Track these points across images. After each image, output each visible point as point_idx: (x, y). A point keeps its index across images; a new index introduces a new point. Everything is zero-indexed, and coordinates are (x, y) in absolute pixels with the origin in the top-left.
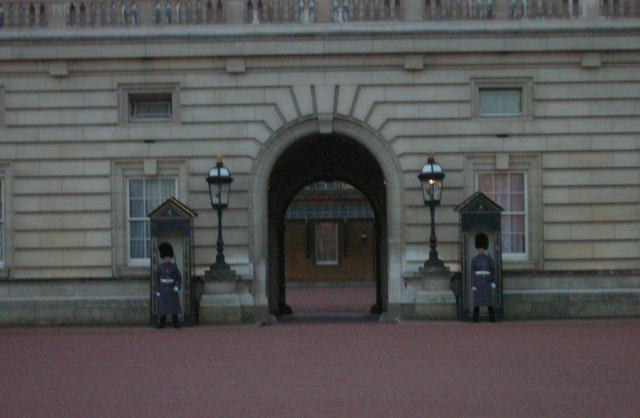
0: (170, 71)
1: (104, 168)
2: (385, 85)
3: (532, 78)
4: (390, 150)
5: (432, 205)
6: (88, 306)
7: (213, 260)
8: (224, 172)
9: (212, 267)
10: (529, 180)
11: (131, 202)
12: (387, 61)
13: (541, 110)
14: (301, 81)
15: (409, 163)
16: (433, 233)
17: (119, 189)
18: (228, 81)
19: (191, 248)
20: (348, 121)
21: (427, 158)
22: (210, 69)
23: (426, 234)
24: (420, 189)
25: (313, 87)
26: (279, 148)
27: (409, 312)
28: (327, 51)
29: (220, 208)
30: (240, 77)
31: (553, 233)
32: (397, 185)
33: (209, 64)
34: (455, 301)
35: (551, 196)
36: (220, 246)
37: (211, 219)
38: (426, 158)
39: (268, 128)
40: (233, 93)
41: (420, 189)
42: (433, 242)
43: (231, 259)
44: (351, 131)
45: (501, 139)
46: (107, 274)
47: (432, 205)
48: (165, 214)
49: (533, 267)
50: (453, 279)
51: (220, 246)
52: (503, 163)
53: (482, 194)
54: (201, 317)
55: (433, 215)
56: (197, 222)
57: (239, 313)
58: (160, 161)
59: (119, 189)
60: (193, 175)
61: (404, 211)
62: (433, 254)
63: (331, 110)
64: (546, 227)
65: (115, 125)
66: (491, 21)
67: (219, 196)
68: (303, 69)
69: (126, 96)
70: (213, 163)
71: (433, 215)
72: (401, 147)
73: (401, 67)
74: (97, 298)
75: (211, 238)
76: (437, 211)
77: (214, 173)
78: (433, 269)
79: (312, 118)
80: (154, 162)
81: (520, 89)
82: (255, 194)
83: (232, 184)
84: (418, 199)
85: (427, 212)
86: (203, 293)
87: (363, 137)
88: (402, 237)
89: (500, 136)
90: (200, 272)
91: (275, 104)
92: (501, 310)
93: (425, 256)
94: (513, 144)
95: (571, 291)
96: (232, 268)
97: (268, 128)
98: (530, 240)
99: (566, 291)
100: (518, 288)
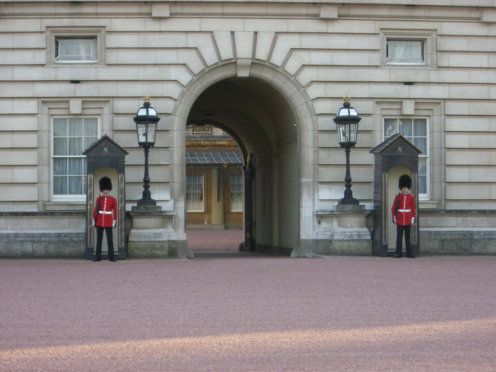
0: (97, 15)
1: (32, 107)
2: (300, 33)
3: (436, 30)
4: (304, 94)
6: (20, 239)
7: (141, 197)
8: (152, 113)
9: (139, 202)
10: (432, 125)
11: (54, 139)
12: (304, 11)
15: (322, 107)
16: (348, 173)
17: (45, 128)
18: (151, 25)
21: (343, 102)
23: (341, 174)
24: (335, 131)
25: (232, 32)
27: (325, 248)
31: (454, 175)
34: (369, 237)
35: (453, 141)
36: (146, 183)
38: (342, 103)
39: (190, 71)
40: (157, 36)
42: (348, 182)
44: (267, 75)
45: (407, 86)
46: (34, 209)
47: (348, 146)
49: (434, 206)
50: (368, 216)
51: (146, 183)
52: (409, 109)
53: (401, 138)
54: (130, 252)
55: (348, 156)
57: (166, 248)
58: (86, 101)
59: (45, 128)
60: (117, 114)
61: (316, 153)
62: (348, 193)
63: (250, 56)
64: (448, 170)
65: (43, 65)
67: (146, 135)
68: (223, 15)
69: (54, 37)
70: (141, 103)
71: (348, 156)
72: (315, 91)
73: (316, 17)
74: (29, 232)
75: (139, 175)
76: (353, 152)
77: (142, 113)
78: (349, 207)
79: (232, 63)
80: (79, 102)
81: (423, 41)
83: (159, 123)
85: (343, 152)
86: (132, 228)
87: (278, 81)
88: (314, 177)
89: (406, 83)
91: (196, 48)
92: (418, 246)
93: (341, 196)
94: (418, 92)
95: (475, 229)
96: (158, 204)
97: (190, 71)
98: (432, 182)
99: (470, 229)
100: (427, 227)
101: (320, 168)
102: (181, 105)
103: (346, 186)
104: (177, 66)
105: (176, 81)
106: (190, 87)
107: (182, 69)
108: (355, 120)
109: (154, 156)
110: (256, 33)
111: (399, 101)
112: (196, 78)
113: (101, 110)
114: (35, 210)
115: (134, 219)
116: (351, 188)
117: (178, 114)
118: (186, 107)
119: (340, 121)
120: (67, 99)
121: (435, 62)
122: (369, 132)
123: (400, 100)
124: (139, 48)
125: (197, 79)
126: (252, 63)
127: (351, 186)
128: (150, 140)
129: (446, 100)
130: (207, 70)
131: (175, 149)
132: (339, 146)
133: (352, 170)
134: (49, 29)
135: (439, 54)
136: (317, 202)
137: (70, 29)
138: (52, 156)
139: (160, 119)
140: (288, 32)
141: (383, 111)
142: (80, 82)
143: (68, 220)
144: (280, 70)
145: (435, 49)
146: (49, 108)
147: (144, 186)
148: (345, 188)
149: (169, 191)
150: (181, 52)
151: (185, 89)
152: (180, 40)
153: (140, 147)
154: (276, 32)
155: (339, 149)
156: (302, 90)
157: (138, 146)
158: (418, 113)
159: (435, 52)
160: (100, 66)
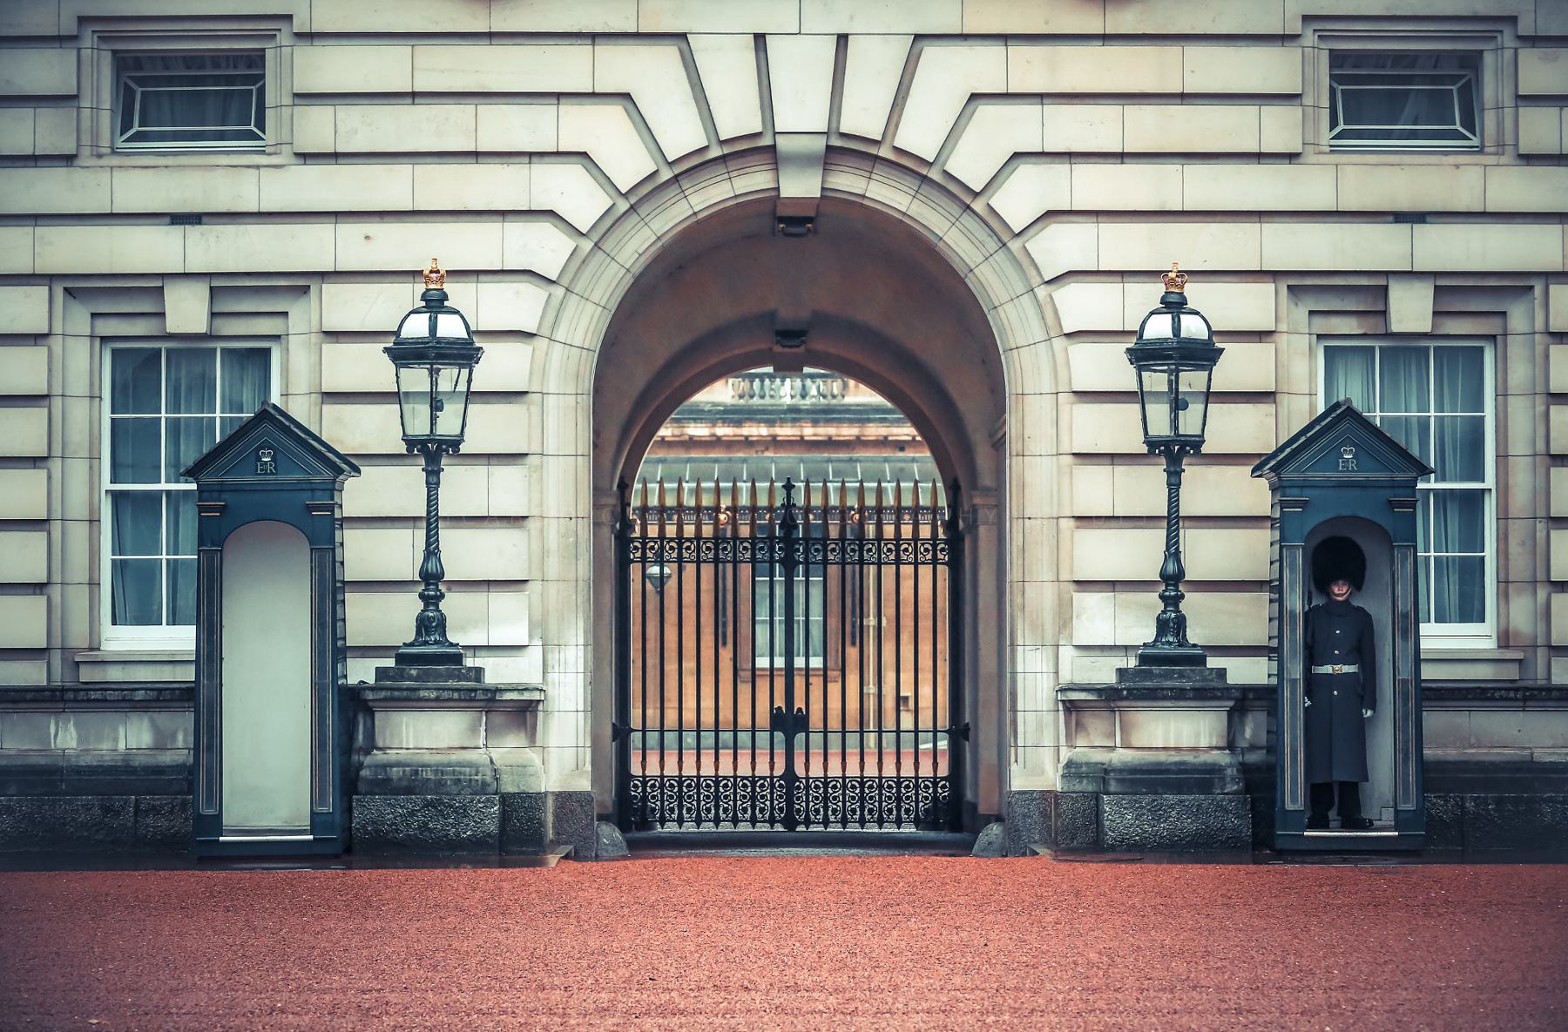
5: (1175, 452)
8: (450, 327)
15: (1084, 305)
16: (1173, 551)
19: (330, 592)
20: (876, 159)
24: (1139, 396)
25: (760, 39)
26: (638, 244)
29: (432, 452)
36: (431, 581)
37: (401, 489)
38: (1157, 290)
41: (1139, 396)
43: (470, 622)
47: (1175, 452)
49: (1511, 672)
51: (431, 581)
56: (357, 496)
62: (1172, 625)
70: (411, 294)
77: (417, 327)
79: (758, 150)
83: (477, 368)
84: (1119, 428)
90: (361, 672)
96: (469, 662)
97: (606, 181)
103: (1161, 597)
105: (551, 213)
107: (576, 170)
108: (1202, 354)
109: (462, 488)
111: (152, 286)
112: (623, 206)
115: (378, 716)
116: (1183, 606)
122: (518, 398)
125: (632, 207)
126: (829, 149)
132: (1145, 449)
136: (1067, 653)
138: (107, 484)
142: (204, 219)
146: (93, 315)
147: (421, 596)
154: (918, 37)
156: (1015, 245)
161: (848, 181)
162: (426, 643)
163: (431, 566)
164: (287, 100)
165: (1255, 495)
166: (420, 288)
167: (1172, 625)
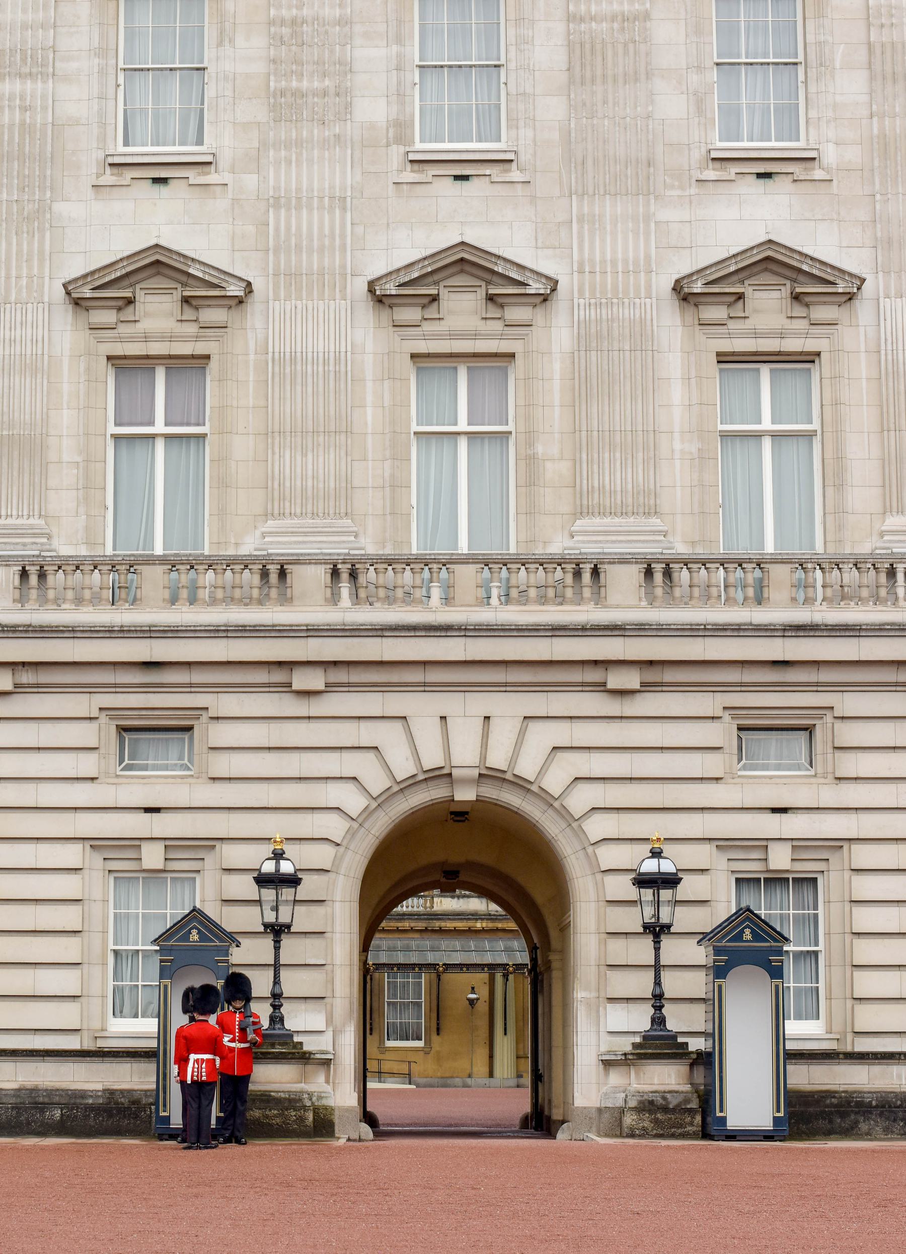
0: (191, 687)
1: (71, 855)
2: (571, 718)
5: (657, 931)
8: (286, 867)
11: (115, 914)
12: (576, 676)
13: (851, 764)
14: (422, 708)
15: (610, 856)
16: (658, 983)
17: (97, 894)
22: (269, 685)
23: (643, 984)
26: (381, 825)
28: (469, 658)
29: (277, 931)
30: (314, 700)
32: (592, 895)
33: (261, 676)
36: (276, 997)
40: (303, 726)
42: (658, 999)
43: (296, 1019)
44: (511, 798)
47: (657, 931)
48: (739, 937)
51: (276, 997)
52: (780, 859)
58: (172, 844)
60: (228, 870)
62: (659, 1021)
65: (93, 779)
66: (759, 608)
67: (276, 909)
68: (425, 687)
70: (267, 850)
76: (666, 942)
77: (269, 867)
80: (159, 847)
81: (809, 730)
82: (337, 905)
84: (632, 920)
85: (649, 941)
89: (775, 810)
93: (644, 1024)
101: (611, 974)
102: (350, 853)
103: (653, 1006)
104: (339, 781)
105: (338, 808)
106: (365, 820)
108: (671, 881)
109: (291, 949)
110: (487, 718)
112: (374, 805)
113: (200, 862)
114: (77, 1047)
116: (663, 1011)
117: (343, 871)
118: (358, 857)
119: (643, 881)
120: (137, 843)
121: (830, 769)
123: (764, 843)
124: (269, 748)
127: (663, 1006)
128: (284, 918)
129: (852, 842)
130: (396, 788)
131: (337, 936)
133: (665, 976)
134: (104, 713)
135: (838, 754)
137: (144, 712)
139: (301, 879)
140: (548, 717)
141: (732, 863)
143: (129, 1065)
144: (534, 788)
145: (830, 745)
147: (272, 1005)
148: (652, 1011)
149: (324, 1012)
150: (346, 755)
151: (355, 825)
152: (346, 734)
153: (265, 932)
155: (262, 936)
156: (575, 825)
157: (262, 929)
158: (799, 866)
159: (830, 750)
160: (200, 780)
161: (490, 792)
162: (274, 1029)
163: (277, 991)
164: (205, 750)
165: (700, 954)
166: (272, 847)
167: (659, 1021)
